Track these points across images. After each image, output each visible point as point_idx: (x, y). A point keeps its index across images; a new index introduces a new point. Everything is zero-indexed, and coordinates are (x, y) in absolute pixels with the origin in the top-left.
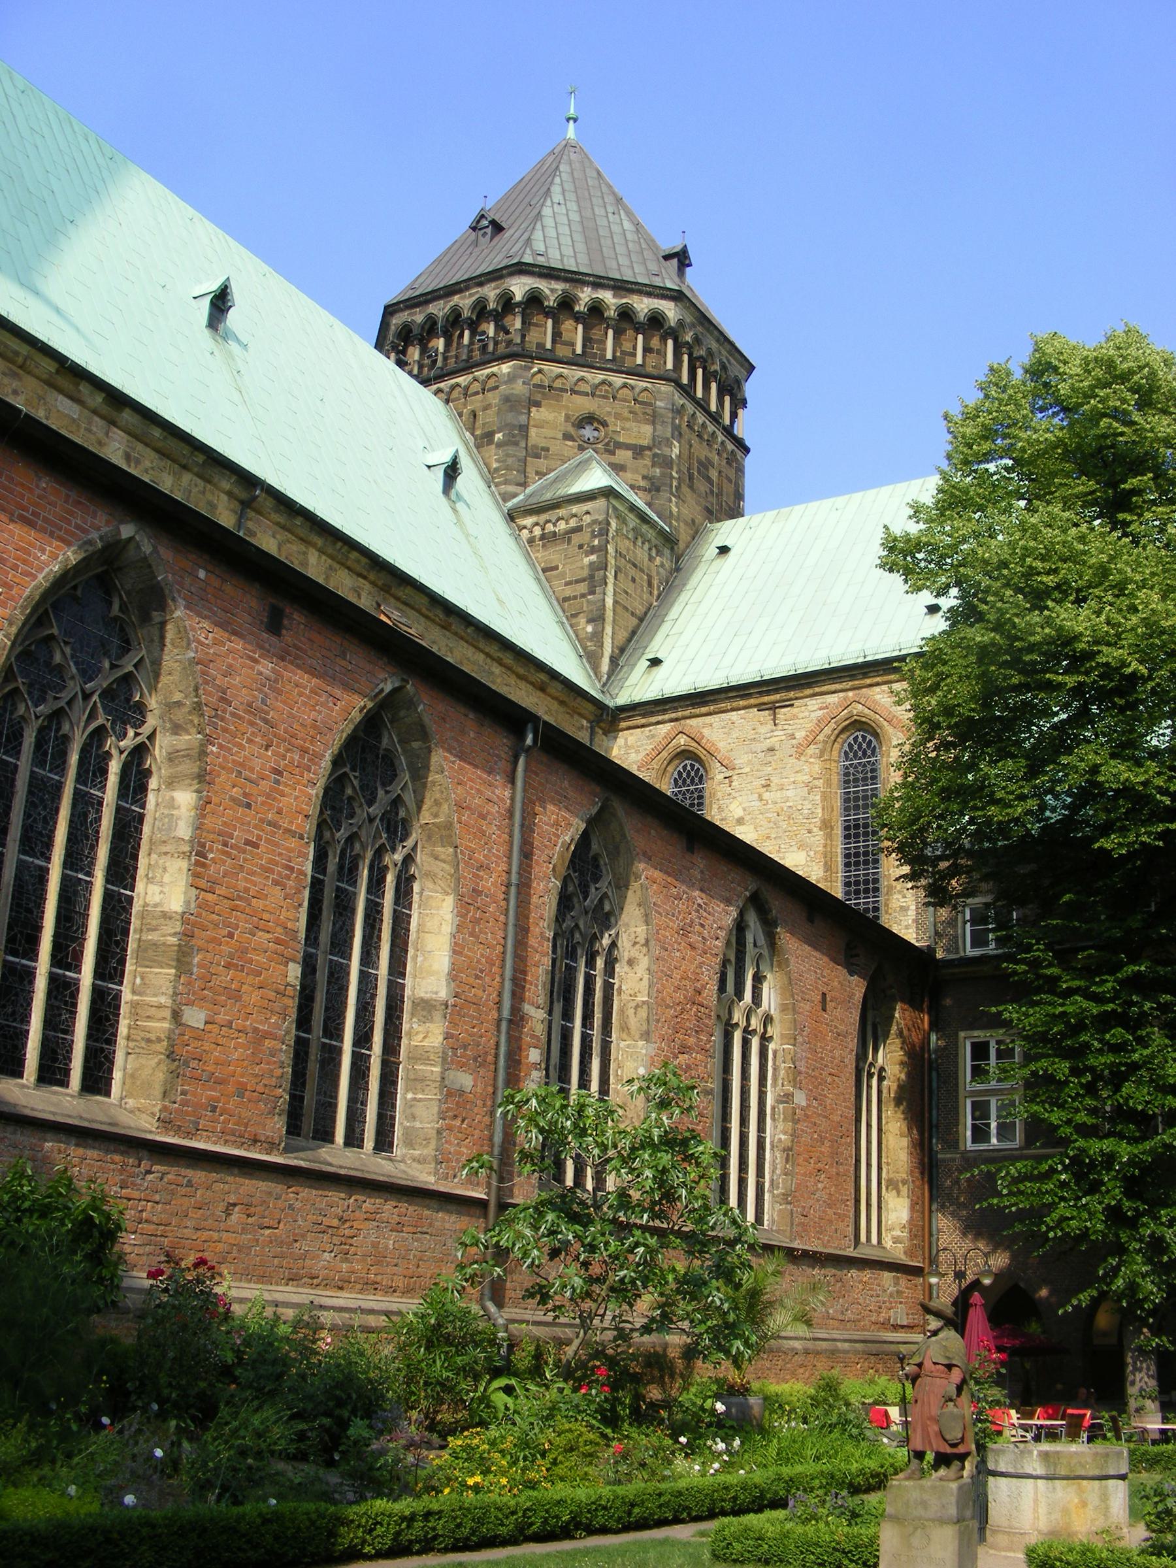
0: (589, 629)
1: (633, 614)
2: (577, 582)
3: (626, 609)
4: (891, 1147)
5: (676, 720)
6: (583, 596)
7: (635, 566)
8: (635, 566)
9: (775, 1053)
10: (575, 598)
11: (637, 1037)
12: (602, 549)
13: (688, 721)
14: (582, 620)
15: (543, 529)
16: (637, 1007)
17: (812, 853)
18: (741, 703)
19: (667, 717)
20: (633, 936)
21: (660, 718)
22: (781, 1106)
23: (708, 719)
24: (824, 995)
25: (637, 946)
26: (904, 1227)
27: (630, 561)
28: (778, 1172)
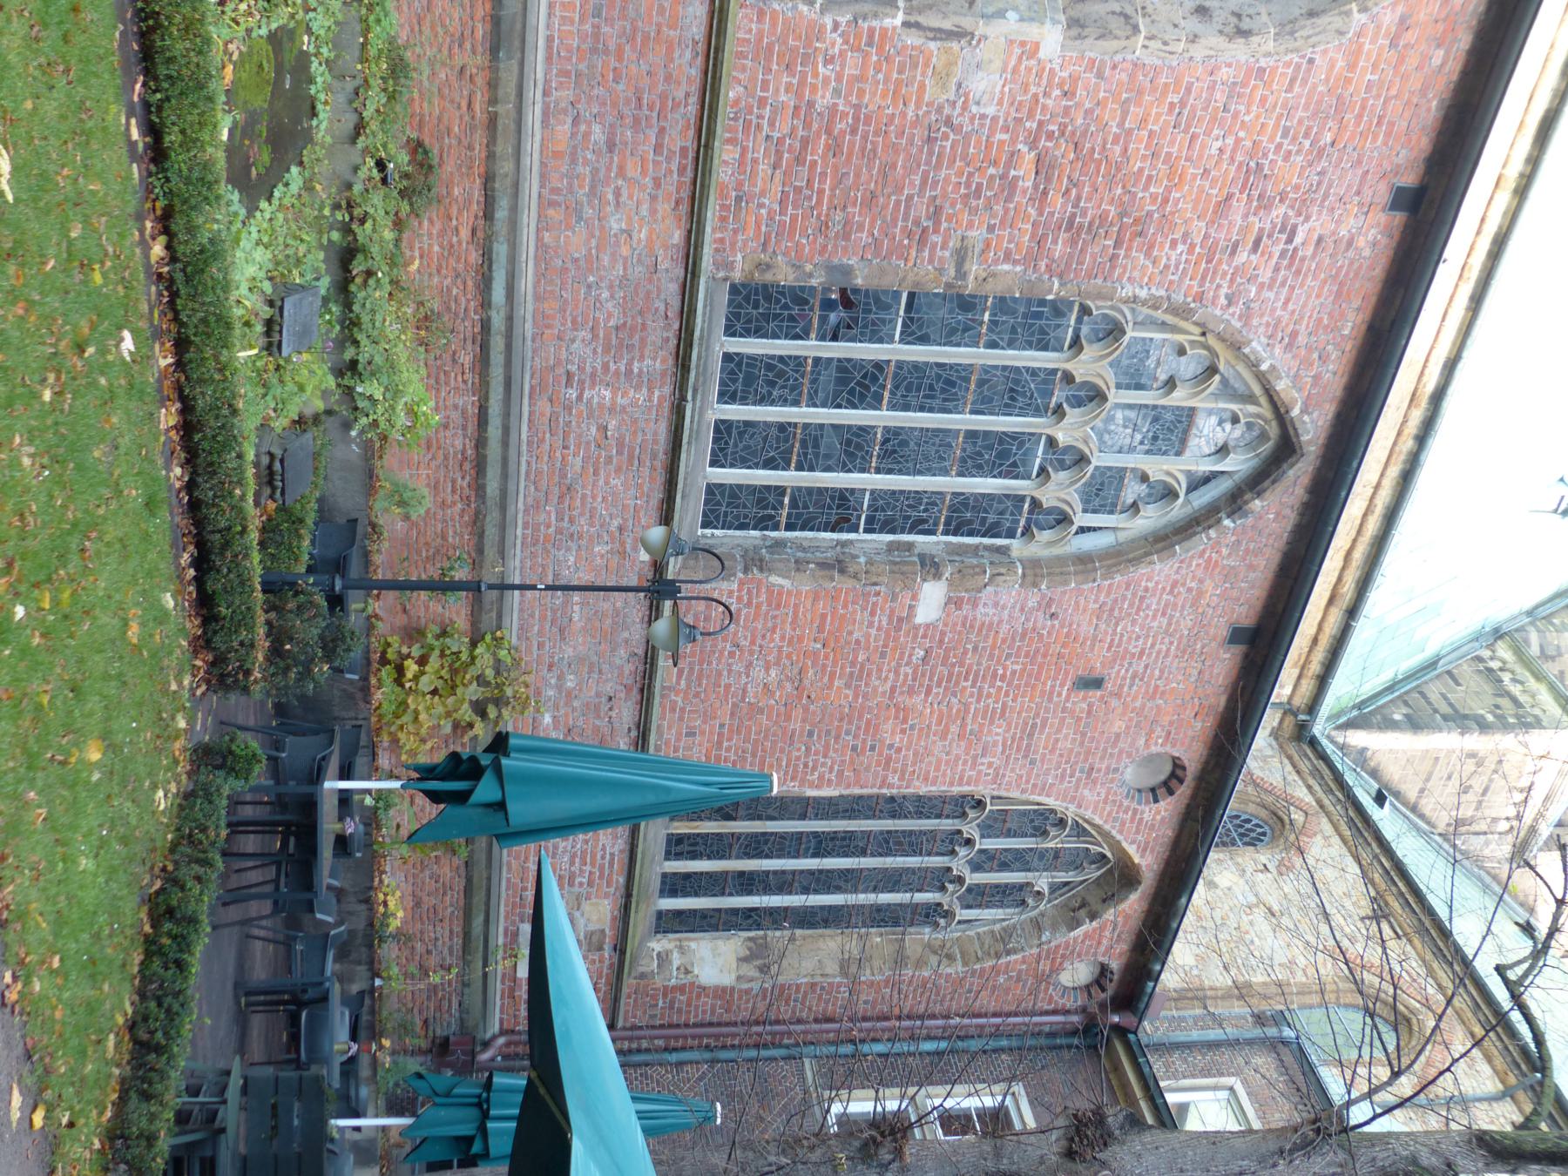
0: (1397, 717)
1: (1422, 791)
2: (1451, 705)
3: (1428, 780)
4: (821, 944)
5: (1322, 806)
6: (1436, 711)
7: (1484, 793)
8: (1484, 793)
9: (1003, 551)
10: (1429, 703)
11: (1071, 13)
12: (1505, 727)
13: (1325, 820)
14: (1405, 710)
15: (1501, 669)
16: (1127, 17)
17: (1195, 972)
18: (1376, 876)
19: (1320, 794)
20: (1251, 11)
21: (1317, 788)
22: (916, 559)
23: (1336, 840)
24: (1097, 683)
25: (1234, 20)
26: (687, 972)
27: (1491, 780)
28: (800, 554)
